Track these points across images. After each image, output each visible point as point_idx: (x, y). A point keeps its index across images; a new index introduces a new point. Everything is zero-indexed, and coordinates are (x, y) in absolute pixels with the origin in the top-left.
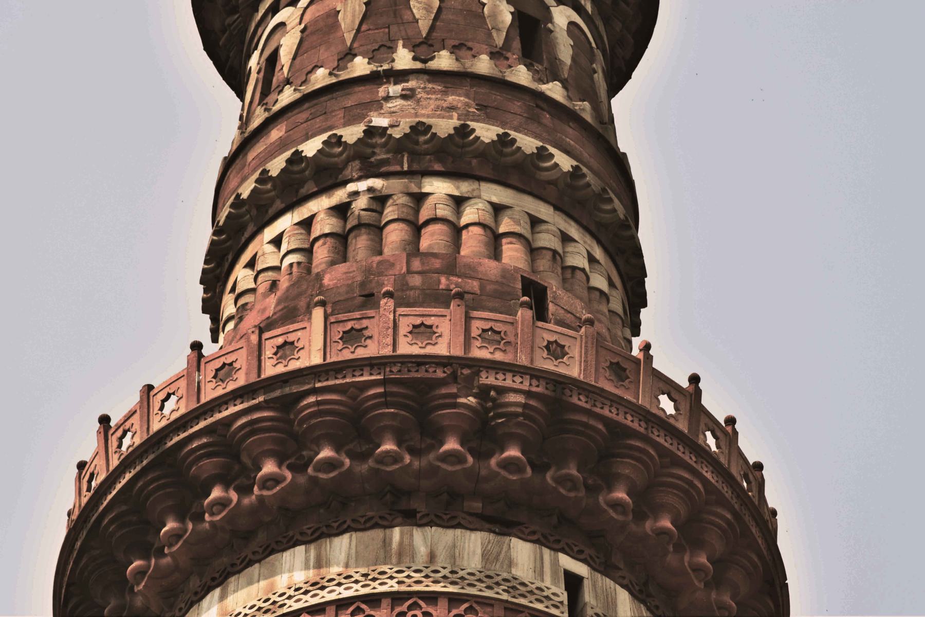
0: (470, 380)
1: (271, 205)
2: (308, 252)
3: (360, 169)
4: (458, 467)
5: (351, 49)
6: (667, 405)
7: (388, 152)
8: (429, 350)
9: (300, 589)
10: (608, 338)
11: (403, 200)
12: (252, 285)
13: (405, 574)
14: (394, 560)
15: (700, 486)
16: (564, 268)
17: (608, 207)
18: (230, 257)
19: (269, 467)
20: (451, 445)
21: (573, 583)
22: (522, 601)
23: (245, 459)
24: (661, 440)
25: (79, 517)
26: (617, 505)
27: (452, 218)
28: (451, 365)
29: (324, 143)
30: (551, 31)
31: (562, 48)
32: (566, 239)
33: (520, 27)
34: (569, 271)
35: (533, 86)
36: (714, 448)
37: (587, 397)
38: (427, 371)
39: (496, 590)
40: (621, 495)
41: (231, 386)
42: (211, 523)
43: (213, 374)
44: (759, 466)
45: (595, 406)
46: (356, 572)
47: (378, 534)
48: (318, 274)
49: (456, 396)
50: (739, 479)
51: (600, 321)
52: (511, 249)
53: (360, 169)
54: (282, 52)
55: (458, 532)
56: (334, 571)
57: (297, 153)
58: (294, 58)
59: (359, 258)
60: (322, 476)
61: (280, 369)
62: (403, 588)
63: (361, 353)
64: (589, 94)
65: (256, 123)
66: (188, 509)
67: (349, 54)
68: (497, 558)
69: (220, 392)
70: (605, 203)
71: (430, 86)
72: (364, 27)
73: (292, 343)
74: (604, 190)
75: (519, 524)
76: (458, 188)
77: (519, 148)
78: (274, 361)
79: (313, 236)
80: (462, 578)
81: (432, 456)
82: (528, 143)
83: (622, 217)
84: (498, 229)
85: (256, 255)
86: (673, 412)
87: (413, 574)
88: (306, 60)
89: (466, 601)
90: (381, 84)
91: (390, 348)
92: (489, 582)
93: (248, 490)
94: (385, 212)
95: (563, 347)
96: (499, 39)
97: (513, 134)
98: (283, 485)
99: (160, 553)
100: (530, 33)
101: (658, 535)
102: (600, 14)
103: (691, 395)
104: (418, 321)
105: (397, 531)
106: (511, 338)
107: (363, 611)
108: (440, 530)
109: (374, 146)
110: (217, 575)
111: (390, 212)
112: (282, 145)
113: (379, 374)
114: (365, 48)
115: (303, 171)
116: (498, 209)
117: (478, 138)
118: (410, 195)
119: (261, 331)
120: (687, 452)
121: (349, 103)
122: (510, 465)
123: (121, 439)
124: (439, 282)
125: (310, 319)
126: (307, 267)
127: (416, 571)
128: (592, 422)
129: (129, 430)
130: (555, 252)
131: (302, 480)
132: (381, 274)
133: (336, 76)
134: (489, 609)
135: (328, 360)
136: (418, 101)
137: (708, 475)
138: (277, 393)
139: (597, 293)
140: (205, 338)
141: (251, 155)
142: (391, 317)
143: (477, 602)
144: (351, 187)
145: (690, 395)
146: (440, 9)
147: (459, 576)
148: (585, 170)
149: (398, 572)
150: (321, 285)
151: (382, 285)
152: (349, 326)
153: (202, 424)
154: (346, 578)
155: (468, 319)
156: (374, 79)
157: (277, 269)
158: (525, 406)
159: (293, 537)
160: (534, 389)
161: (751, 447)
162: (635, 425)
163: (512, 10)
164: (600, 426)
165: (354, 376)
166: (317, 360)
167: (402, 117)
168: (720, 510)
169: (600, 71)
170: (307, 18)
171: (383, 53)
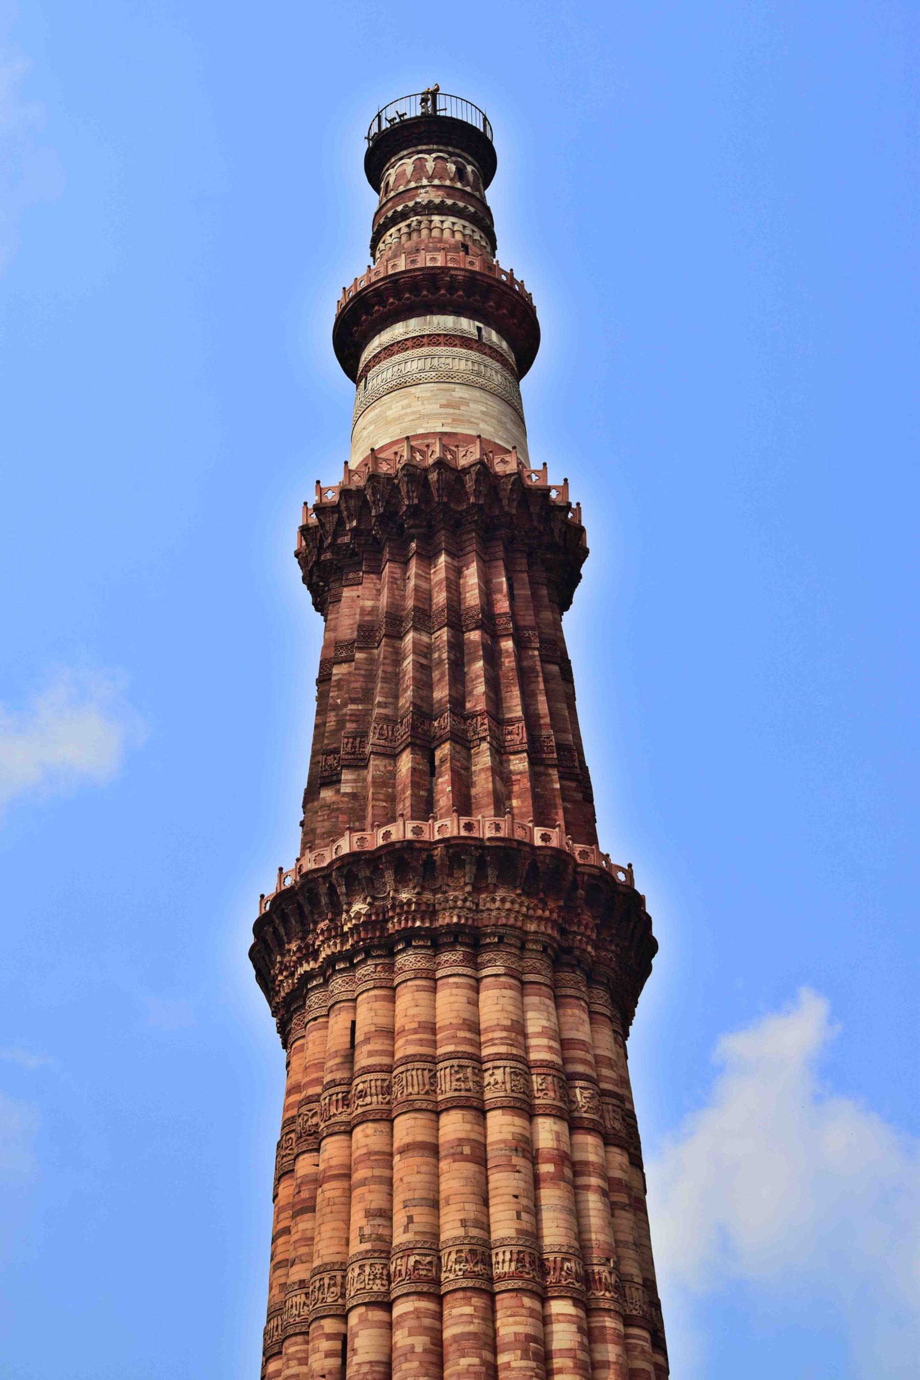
0: (447, 273)
2: (400, 238)
6: (504, 278)
19: (391, 300)
20: (443, 292)
21: (479, 329)
26: (491, 307)
40: (492, 304)
44: (530, 294)
47: (423, 318)
63: (416, 266)
64: (479, 190)
67: (409, 181)
70: (482, 220)
82: (461, 204)
96: (452, 175)
111: (423, 226)
116: (454, 224)
122: (459, 296)
140: (371, 264)
145: (510, 275)
156: (417, 188)
161: (528, 289)
166: (403, 269)
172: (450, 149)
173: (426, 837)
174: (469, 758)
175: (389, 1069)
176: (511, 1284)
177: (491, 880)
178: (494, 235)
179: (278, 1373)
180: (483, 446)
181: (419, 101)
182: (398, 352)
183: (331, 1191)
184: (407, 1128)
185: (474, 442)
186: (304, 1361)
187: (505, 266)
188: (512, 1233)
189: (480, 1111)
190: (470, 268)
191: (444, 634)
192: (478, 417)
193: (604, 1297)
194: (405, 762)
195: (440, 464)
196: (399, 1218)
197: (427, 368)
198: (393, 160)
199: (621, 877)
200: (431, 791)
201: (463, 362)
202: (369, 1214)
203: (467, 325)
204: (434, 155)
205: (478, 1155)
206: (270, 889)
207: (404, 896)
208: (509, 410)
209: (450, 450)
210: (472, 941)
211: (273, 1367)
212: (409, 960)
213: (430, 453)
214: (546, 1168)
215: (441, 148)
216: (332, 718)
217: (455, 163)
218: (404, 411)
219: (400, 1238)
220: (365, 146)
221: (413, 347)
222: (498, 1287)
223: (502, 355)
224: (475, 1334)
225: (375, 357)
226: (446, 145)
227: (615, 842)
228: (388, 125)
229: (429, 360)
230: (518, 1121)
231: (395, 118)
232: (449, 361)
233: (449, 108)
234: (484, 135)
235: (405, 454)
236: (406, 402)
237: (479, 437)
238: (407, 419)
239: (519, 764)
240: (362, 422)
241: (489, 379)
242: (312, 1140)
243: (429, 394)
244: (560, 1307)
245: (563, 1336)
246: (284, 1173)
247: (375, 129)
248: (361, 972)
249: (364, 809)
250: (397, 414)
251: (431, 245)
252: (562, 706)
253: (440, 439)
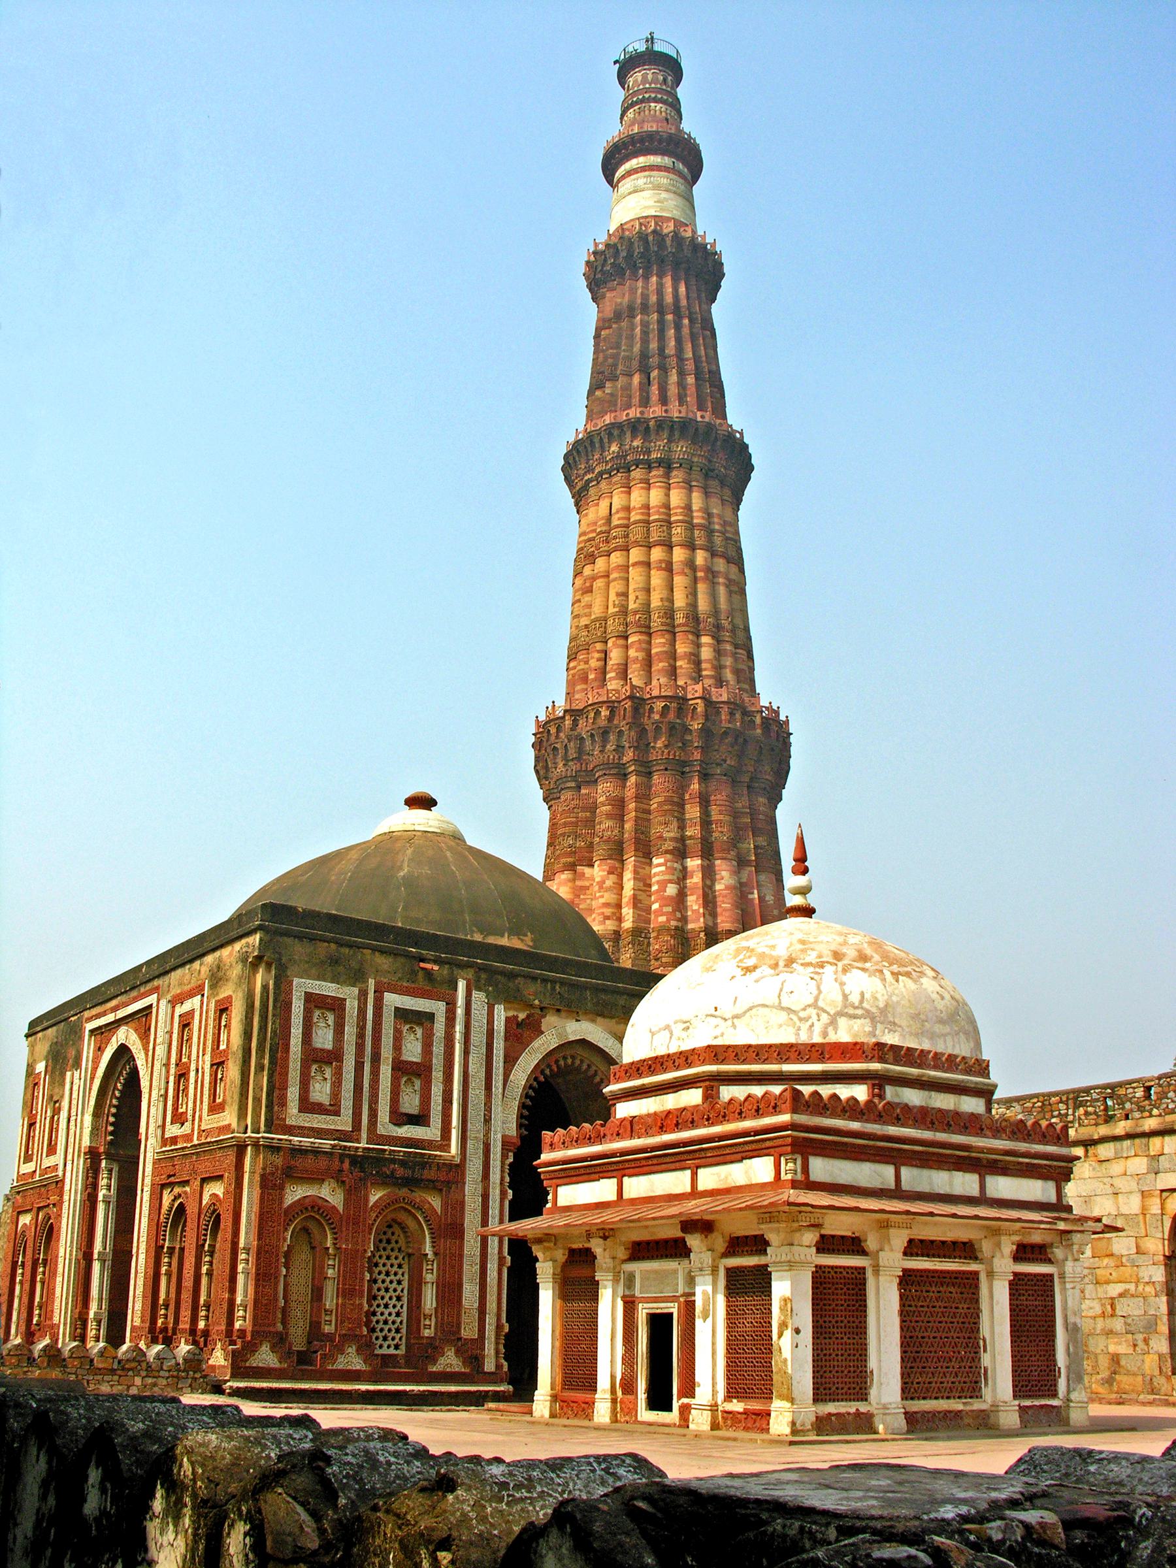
70: (675, 105)
145: (689, 135)
173: (646, 416)
174: (667, 377)
175: (627, 526)
176: (683, 629)
177: (677, 436)
179: (574, 668)
183: (599, 584)
184: (636, 554)
186: (587, 662)
187: (687, 130)
188: (683, 604)
189: (670, 547)
191: (655, 316)
192: (671, 207)
193: (726, 635)
194: (636, 379)
195: (654, 232)
196: (632, 597)
199: (738, 435)
200: (648, 393)
202: (618, 595)
203: (667, 161)
205: (669, 568)
206: (572, 440)
207: (635, 444)
210: (667, 465)
211: (572, 665)
212: (637, 474)
214: (700, 574)
216: (601, 355)
219: (632, 606)
222: (677, 630)
224: (666, 652)
227: (735, 418)
230: (687, 552)
233: (658, 47)
239: (691, 380)
242: (591, 558)
244: (705, 640)
245: (706, 653)
246: (577, 574)
248: (615, 479)
249: (616, 401)
252: (711, 353)
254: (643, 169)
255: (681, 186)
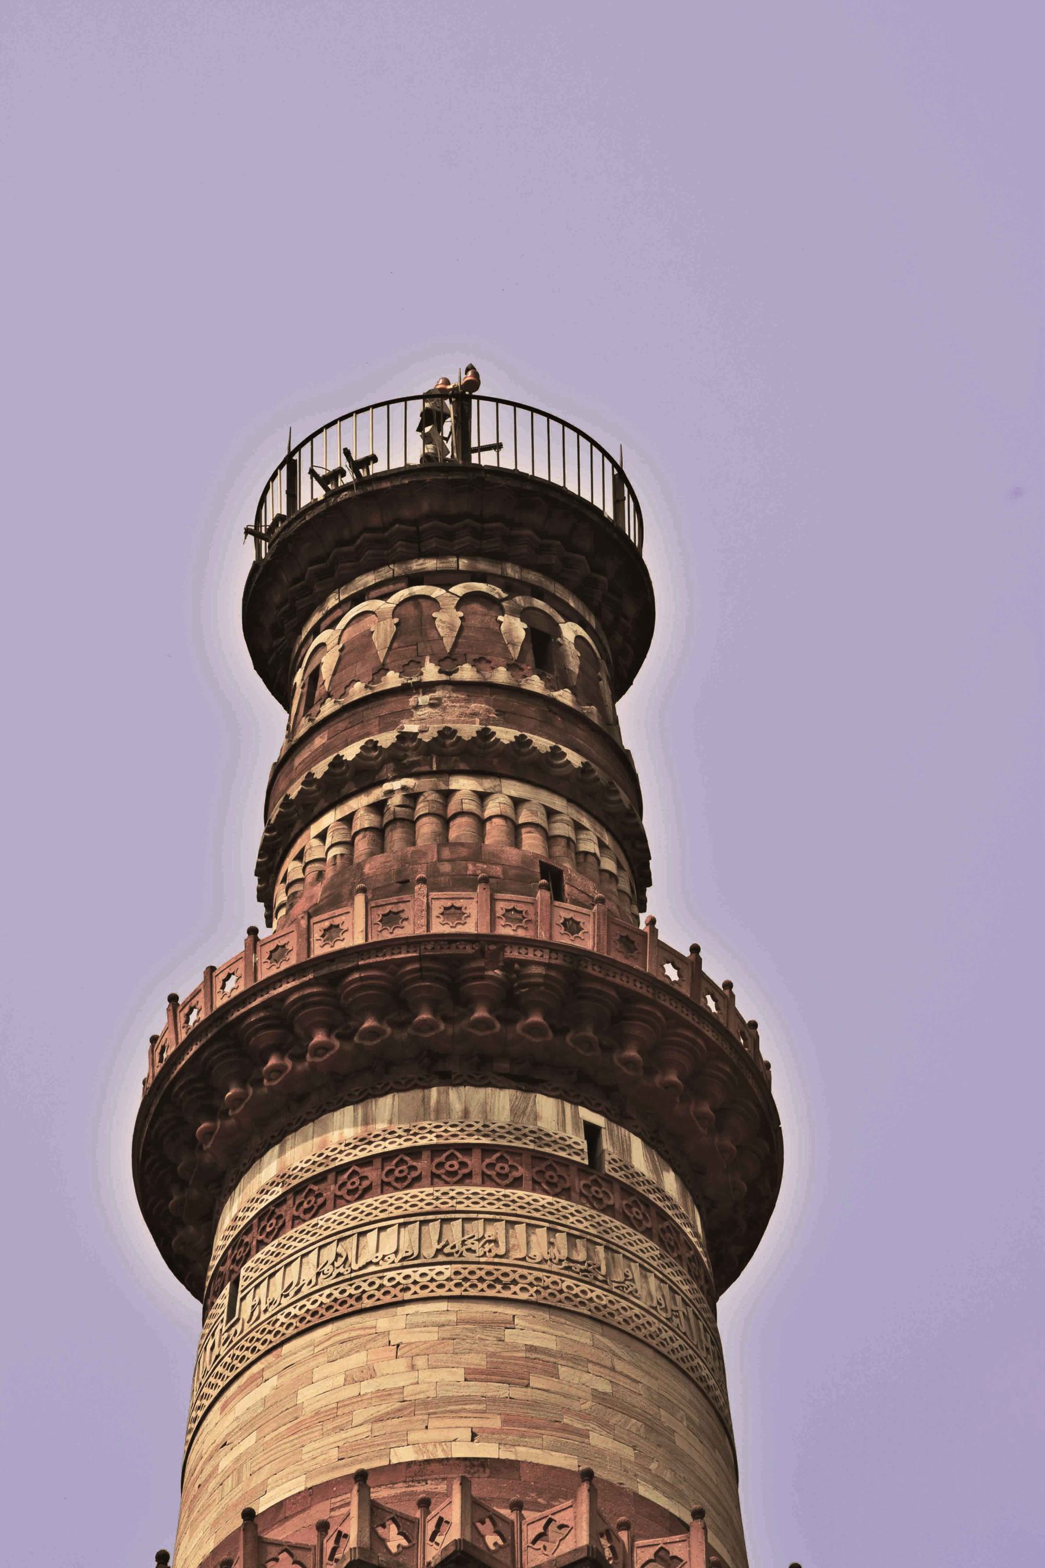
1: (315, 805)
2: (350, 844)
3: (394, 771)
4: (487, 1033)
5: (383, 664)
6: (671, 973)
7: (419, 754)
8: (460, 929)
9: (349, 1144)
10: (618, 914)
11: (434, 796)
12: (301, 876)
13: (442, 1129)
14: (432, 1117)
15: (702, 1044)
16: (578, 853)
17: (614, 798)
18: (281, 851)
19: (319, 1037)
20: (481, 1013)
21: (592, 1132)
22: (547, 1150)
23: (298, 1030)
24: (667, 1004)
25: (153, 1084)
26: (628, 1062)
27: (477, 811)
28: (478, 941)
29: (361, 748)
30: (561, 645)
31: (571, 659)
32: (578, 827)
33: (533, 641)
34: (581, 858)
35: (546, 693)
36: (714, 1010)
37: (601, 967)
38: (457, 948)
39: (524, 1140)
40: (632, 1053)
41: (284, 966)
42: (270, 1088)
43: (268, 956)
44: (754, 1025)
45: (608, 975)
46: (399, 1128)
47: (417, 1094)
48: (359, 864)
49: (483, 969)
50: (736, 1036)
51: (610, 899)
52: (530, 838)
53: (394, 771)
54: (323, 669)
55: (489, 1090)
56: (380, 1127)
57: (339, 758)
58: (334, 674)
59: (395, 848)
60: (367, 1043)
61: (328, 949)
62: (442, 1141)
63: (399, 933)
64: (596, 699)
65: (301, 732)
66: (249, 1076)
67: (383, 669)
68: (524, 1113)
69: (274, 971)
71: (455, 695)
72: (395, 645)
73: (338, 926)
74: (611, 783)
75: (542, 1081)
76: (481, 785)
77: (535, 748)
78: (321, 943)
79: (354, 831)
80: (494, 1131)
81: (464, 1024)
82: (542, 743)
83: (627, 806)
84: (517, 819)
85: (303, 849)
86: (677, 979)
87: (450, 1129)
88: (345, 675)
89: (496, 1151)
90: (411, 695)
91: (425, 928)
92: (518, 1134)
93: (301, 1058)
94: (418, 807)
95: (578, 923)
96: (515, 653)
97: (529, 736)
98: (332, 1052)
99: (225, 1115)
100: (542, 646)
101: (666, 1088)
102: (604, 629)
103: (692, 963)
104: (449, 904)
105: (434, 1090)
106: (532, 917)
107: (407, 1163)
108: (472, 1089)
109: (406, 750)
110: (276, 1134)
111: (421, 808)
112: (325, 751)
113: (415, 951)
114: (397, 663)
115: (344, 773)
116: (517, 803)
117: (497, 740)
118: (439, 791)
119: (310, 917)
120: (690, 1013)
121: (385, 712)
122: (533, 1028)
123: (188, 1015)
124: (467, 868)
125: (353, 904)
126: (349, 858)
127: (452, 1126)
128: (606, 989)
129: (195, 1007)
130: (569, 839)
131: (348, 1047)
132: (415, 863)
133: (371, 688)
134: (517, 1158)
135: (370, 941)
136: (445, 709)
137: (710, 1034)
138: (325, 971)
139: (607, 875)
140: (260, 923)
141: (298, 761)
142: (425, 900)
143: (508, 1152)
144: (387, 786)
145: (691, 964)
146: (461, 628)
147: (490, 1129)
148: (593, 766)
149: (436, 1127)
150: (362, 874)
151: (417, 872)
152: (388, 909)
153: (259, 1001)
154: (390, 1133)
155: (493, 901)
156: (405, 690)
157: (323, 860)
158: (546, 976)
159: (342, 1099)
160: (553, 962)
161: (746, 1008)
162: (644, 991)
163: (526, 626)
164: (613, 993)
165: (393, 954)
166: (359, 940)
167: (431, 723)
168: (721, 1065)
169: (605, 679)
170: (345, 638)
171: (412, 668)
172: (511, 571)
178: (641, 837)
180: (602, 1506)
181: (415, 420)
182: (338, 1201)
185: (571, 1494)
187: (675, 936)
190: (566, 940)
192: (582, 1405)
197: (428, 1252)
198: (332, 602)
201: (541, 1234)
204: (459, 590)
208: (681, 1391)
209: (495, 1519)
213: (431, 1527)
215: (483, 566)
217: (524, 614)
218: (352, 1391)
220: (243, 557)
221: (384, 1186)
223: (662, 1216)
225: (263, 1215)
226: (498, 557)
228: (320, 493)
229: (433, 1228)
231: (341, 472)
232: (497, 1230)
233: (506, 444)
234: (615, 527)
235: (352, 1529)
236: (357, 1360)
237: (588, 1475)
238: (360, 1415)
240: (217, 1426)
241: (624, 1291)
243: (432, 1336)
247: (277, 505)
250: (333, 1398)
251: (446, 868)
253: (465, 1483)
254: (399, 1168)
255: (650, 1285)
